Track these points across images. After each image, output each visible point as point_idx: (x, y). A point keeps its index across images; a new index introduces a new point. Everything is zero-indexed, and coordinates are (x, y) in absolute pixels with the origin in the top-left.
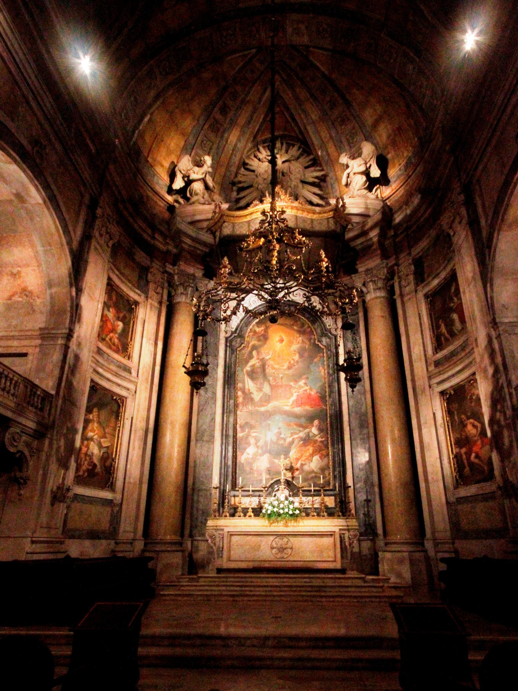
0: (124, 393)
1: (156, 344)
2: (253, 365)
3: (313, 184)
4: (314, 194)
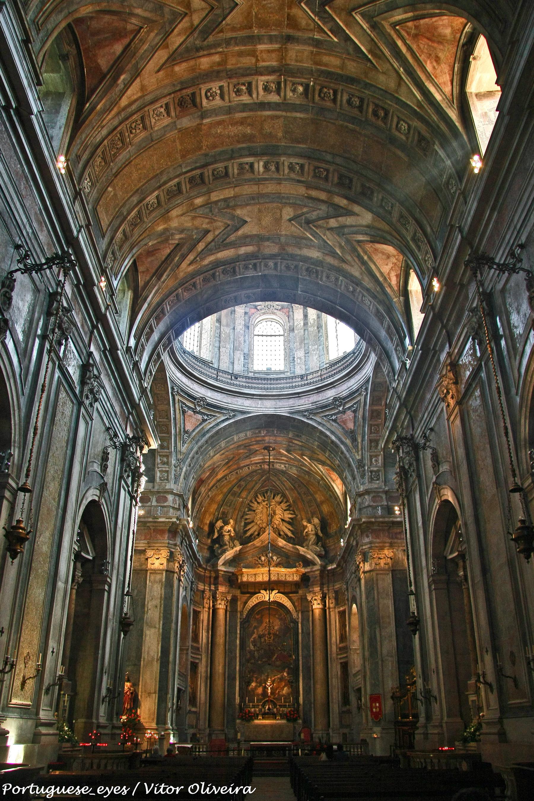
0: (197, 661)
1: (208, 632)
2: (254, 638)
3: (289, 523)
4: (289, 529)
